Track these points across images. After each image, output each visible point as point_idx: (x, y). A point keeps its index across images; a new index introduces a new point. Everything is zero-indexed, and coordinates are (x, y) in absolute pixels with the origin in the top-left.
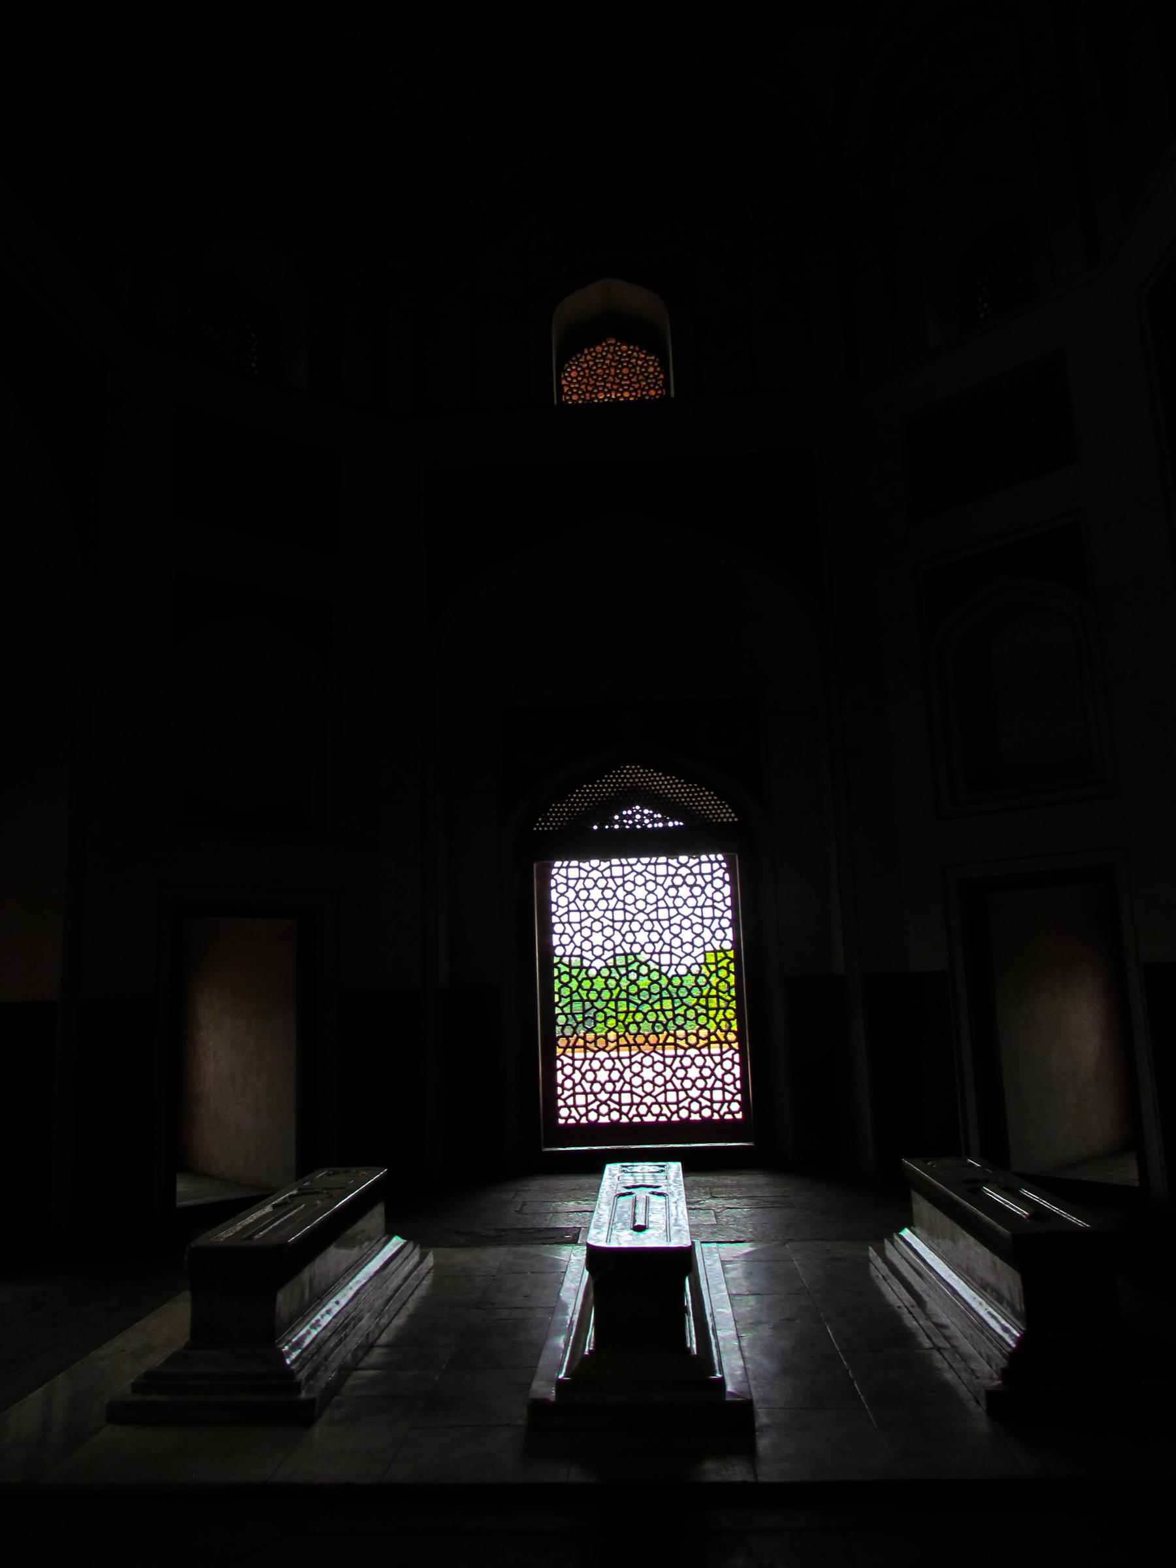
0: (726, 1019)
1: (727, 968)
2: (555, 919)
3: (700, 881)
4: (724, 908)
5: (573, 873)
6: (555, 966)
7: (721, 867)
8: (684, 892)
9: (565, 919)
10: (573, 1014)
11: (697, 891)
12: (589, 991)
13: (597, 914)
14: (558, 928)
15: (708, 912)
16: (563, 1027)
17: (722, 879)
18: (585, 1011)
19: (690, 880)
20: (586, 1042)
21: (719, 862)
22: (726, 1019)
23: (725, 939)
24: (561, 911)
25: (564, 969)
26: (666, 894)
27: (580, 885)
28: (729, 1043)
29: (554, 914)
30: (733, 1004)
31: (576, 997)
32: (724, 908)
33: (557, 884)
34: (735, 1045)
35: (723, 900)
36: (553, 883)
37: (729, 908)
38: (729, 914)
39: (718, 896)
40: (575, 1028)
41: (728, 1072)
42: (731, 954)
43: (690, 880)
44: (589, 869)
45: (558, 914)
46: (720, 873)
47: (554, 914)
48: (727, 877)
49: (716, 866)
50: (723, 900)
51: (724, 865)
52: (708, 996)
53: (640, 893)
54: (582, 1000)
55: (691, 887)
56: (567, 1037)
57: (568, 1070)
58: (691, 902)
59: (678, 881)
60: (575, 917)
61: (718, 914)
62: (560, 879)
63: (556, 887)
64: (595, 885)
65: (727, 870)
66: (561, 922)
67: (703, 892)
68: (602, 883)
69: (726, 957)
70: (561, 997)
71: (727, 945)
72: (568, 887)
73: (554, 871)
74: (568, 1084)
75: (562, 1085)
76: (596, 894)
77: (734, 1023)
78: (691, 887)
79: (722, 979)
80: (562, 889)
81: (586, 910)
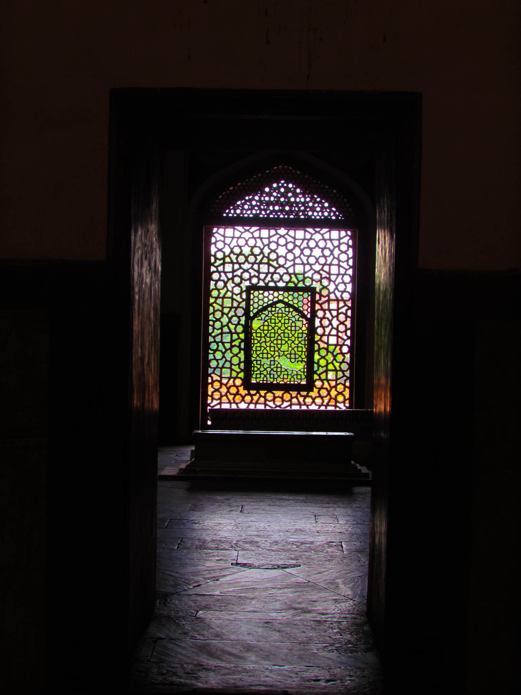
1: (346, 314)
2: (213, 269)
3: (329, 245)
4: (347, 267)
6: (211, 305)
7: (347, 235)
8: (317, 252)
9: (221, 269)
10: (223, 343)
11: (327, 252)
12: (236, 325)
13: (246, 266)
14: (215, 276)
18: (232, 341)
19: (322, 244)
20: (232, 364)
23: (345, 291)
24: (218, 262)
25: (217, 307)
26: (302, 253)
27: (234, 243)
28: (343, 372)
29: (213, 264)
30: (348, 342)
31: (225, 329)
32: (347, 267)
33: (217, 241)
34: (347, 374)
35: (347, 261)
36: (213, 240)
37: (350, 267)
38: (350, 272)
39: (343, 257)
40: (224, 353)
41: (340, 393)
43: (322, 244)
45: (216, 264)
46: (345, 240)
47: (213, 264)
48: (350, 243)
50: (347, 261)
53: (282, 251)
54: (230, 332)
56: (217, 360)
57: (217, 385)
59: (312, 244)
60: (228, 268)
61: (342, 271)
62: (219, 237)
63: (215, 243)
64: (247, 244)
65: (351, 237)
66: (217, 271)
67: (332, 254)
70: (214, 328)
71: (346, 296)
72: (225, 244)
74: (217, 395)
75: (212, 396)
76: (246, 250)
77: (348, 356)
81: (238, 263)
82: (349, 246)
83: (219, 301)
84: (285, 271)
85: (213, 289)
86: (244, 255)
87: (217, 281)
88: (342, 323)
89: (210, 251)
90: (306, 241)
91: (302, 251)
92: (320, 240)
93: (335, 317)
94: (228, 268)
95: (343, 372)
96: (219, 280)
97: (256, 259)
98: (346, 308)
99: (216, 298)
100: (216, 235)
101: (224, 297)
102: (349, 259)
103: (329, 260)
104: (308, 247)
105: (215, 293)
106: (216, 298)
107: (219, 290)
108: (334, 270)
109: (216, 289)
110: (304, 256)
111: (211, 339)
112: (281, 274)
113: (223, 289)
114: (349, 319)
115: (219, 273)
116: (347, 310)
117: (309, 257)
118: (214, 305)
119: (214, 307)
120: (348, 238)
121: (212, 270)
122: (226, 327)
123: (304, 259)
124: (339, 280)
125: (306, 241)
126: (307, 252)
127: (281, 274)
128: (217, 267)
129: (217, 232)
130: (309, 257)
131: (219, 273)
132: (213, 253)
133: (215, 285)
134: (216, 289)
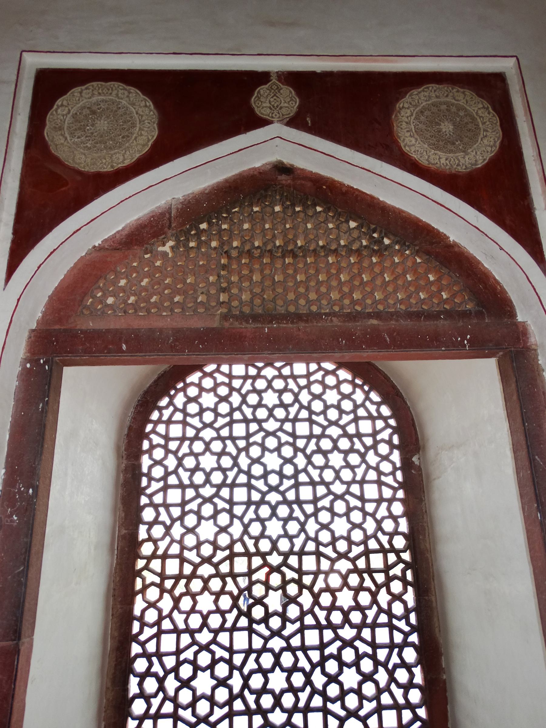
0: (403, 664)
5: (176, 431)
6: (139, 573)
7: (388, 426)
9: (158, 499)
11: (354, 459)
14: (148, 514)
15: (371, 491)
16: (142, 677)
17: (389, 442)
21: (385, 419)
22: (403, 664)
23: (396, 532)
24: (155, 486)
25: (150, 578)
26: (310, 462)
27: (185, 449)
28: (412, 708)
35: (393, 473)
36: (146, 445)
42: (406, 556)
44: (200, 425)
46: (385, 435)
48: (396, 440)
49: (380, 424)
50: (393, 473)
51: (392, 422)
52: (374, 626)
55: (346, 453)
58: (347, 475)
59: (326, 444)
60: (174, 496)
62: (156, 440)
63: (150, 451)
65: (396, 430)
67: (364, 461)
68: (217, 446)
69: (400, 560)
70: (143, 624)
73: (149, 427)
77: (417, 671)
78: (346, 453)
79: (397, 597)
80: (158, 454)
82: (392, 447)
83: (156, 565)
84: (280, 498)
85: (144, 541)
86: (203, 470)
87: (151, 525)
88: (397, 597)
89: (140, 466)
90: (314, 441)
91: (309, 458)
92: (340, 436)
93: (382, 587)
94: (174, 496)
95: (412, 708)
96: (156, 522)
97: (226, 477)
98: (401, 566)
99: (149, 559)
100: (152, 436)
101: (165, 557)
102: (395, 469)
103: (360, 472)
104: (319, 450)
105: (147, 549)
106: (149, 559)
107: (155, 542)
108: (371, 491)
109: (150, 539)
110: (315, 467)
111: (136, 649)
112: (273, 503)
113: (162, 539)
114: (410, 589)
115: (156, 507)
116: (404, 571)
117: (322, 469)
118: (145, 573)
119: (144, 579)
120: (389, 431)
121: (142, 504)
122: (168, 620)
123: (315, 474)
124: (382, 512)
125: (314, 441)
126: (318, 460)
127: (273, 503)
128: (150, 496)
129: (153, 431)
130: (322, 469)
131: (156, 507)
132: (145, 470)
133: (148, 531)
134: (150, 539)
